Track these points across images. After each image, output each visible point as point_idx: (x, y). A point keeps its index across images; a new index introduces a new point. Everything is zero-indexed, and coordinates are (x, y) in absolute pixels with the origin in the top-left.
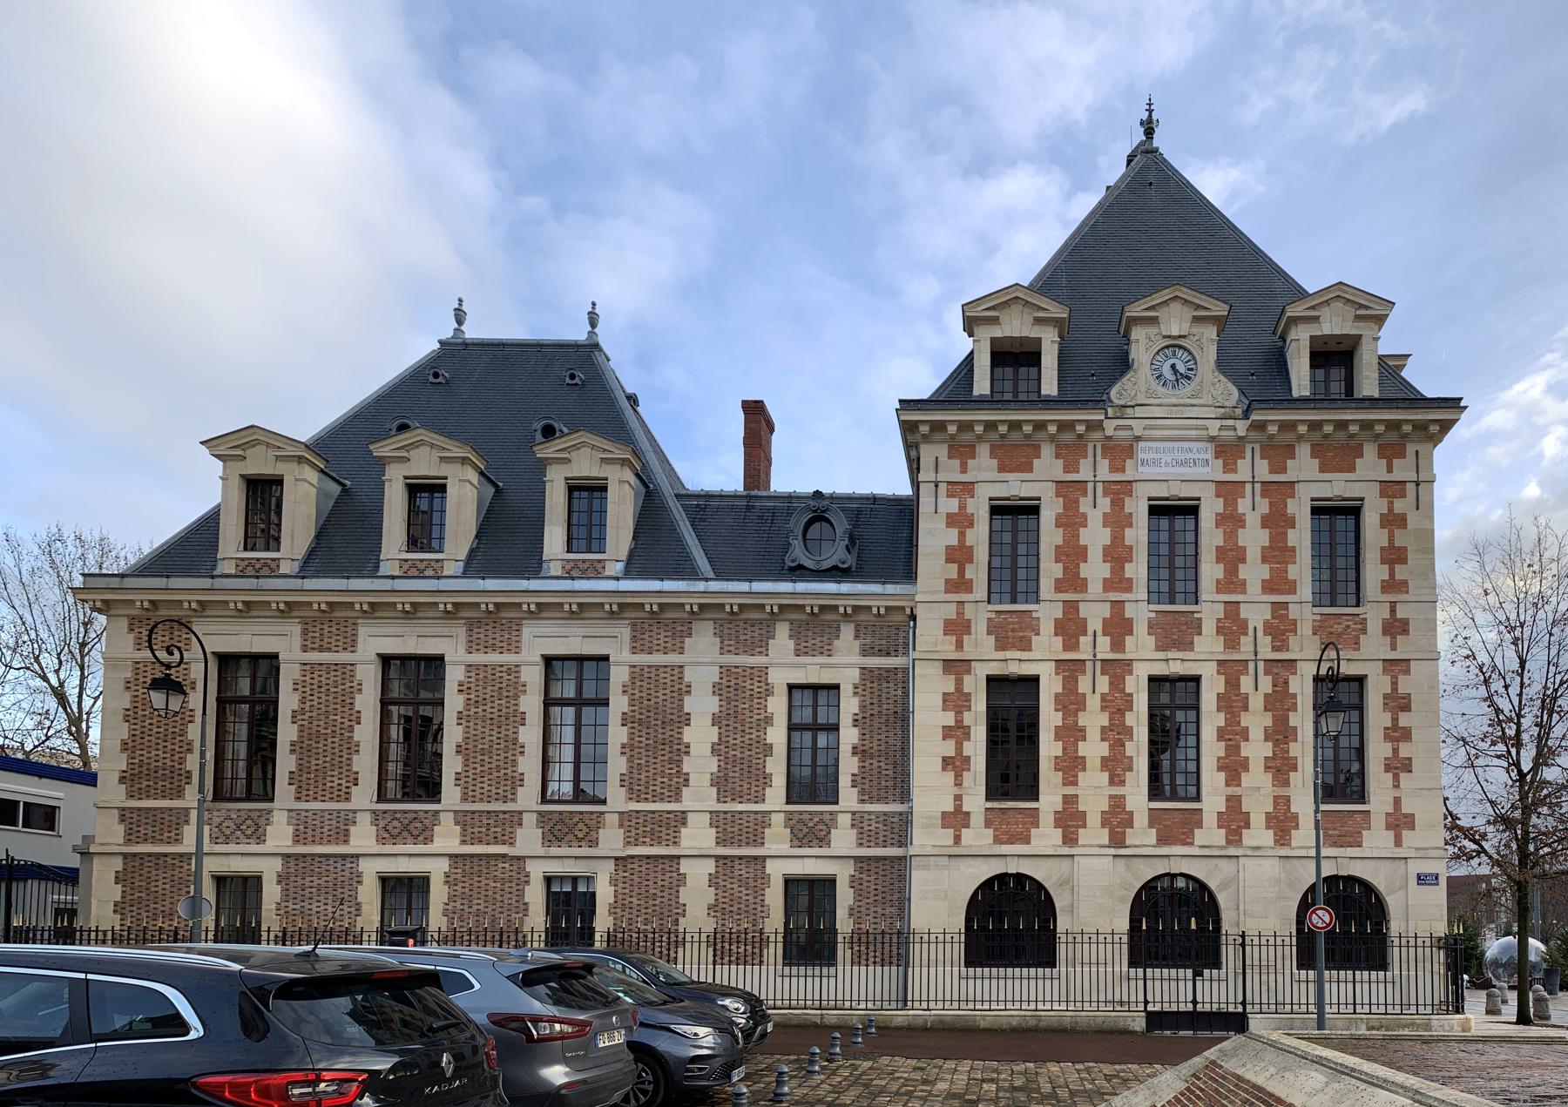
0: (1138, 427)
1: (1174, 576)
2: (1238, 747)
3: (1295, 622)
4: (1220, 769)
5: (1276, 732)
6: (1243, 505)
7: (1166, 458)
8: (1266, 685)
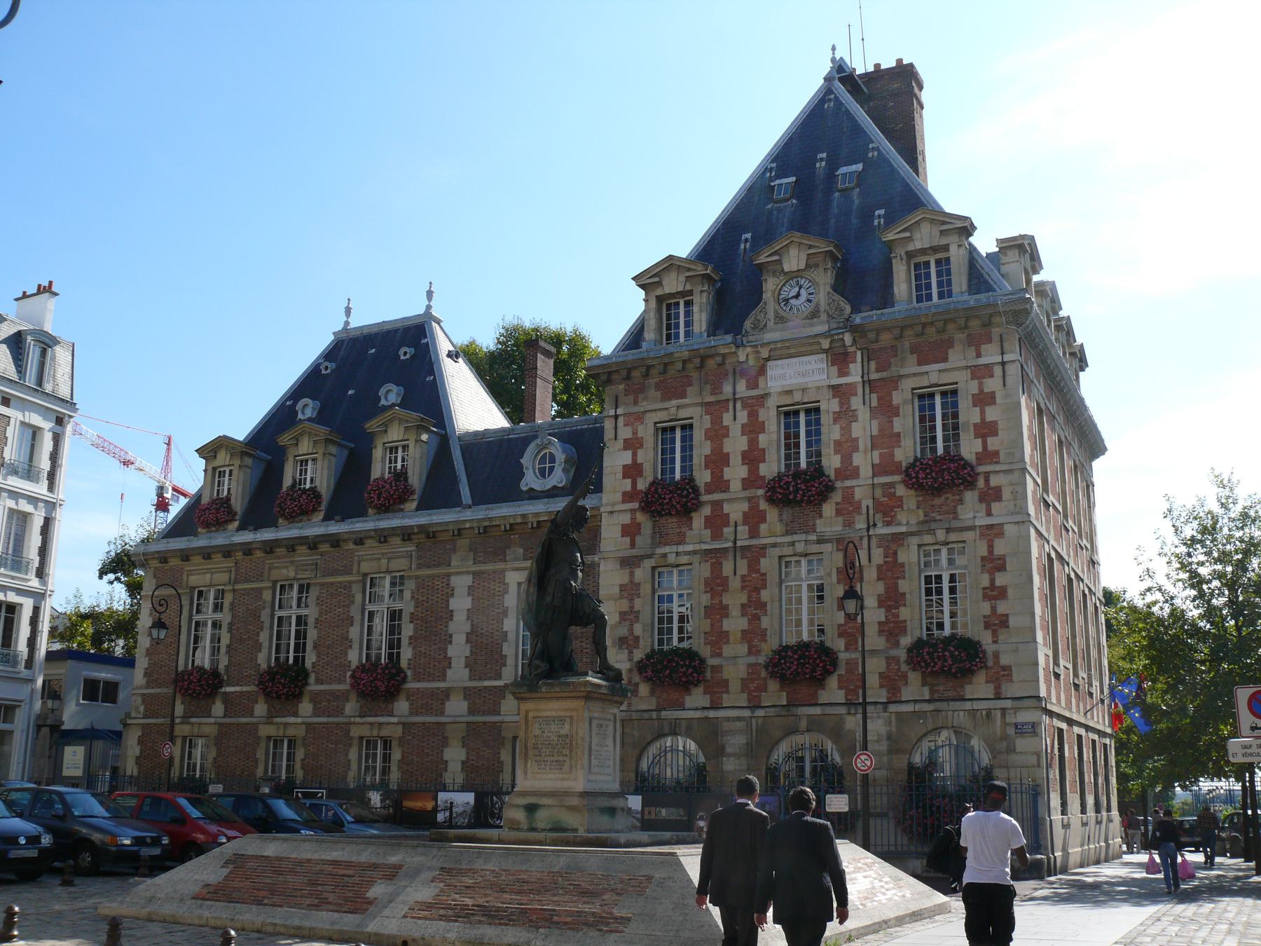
6: (856, 402)
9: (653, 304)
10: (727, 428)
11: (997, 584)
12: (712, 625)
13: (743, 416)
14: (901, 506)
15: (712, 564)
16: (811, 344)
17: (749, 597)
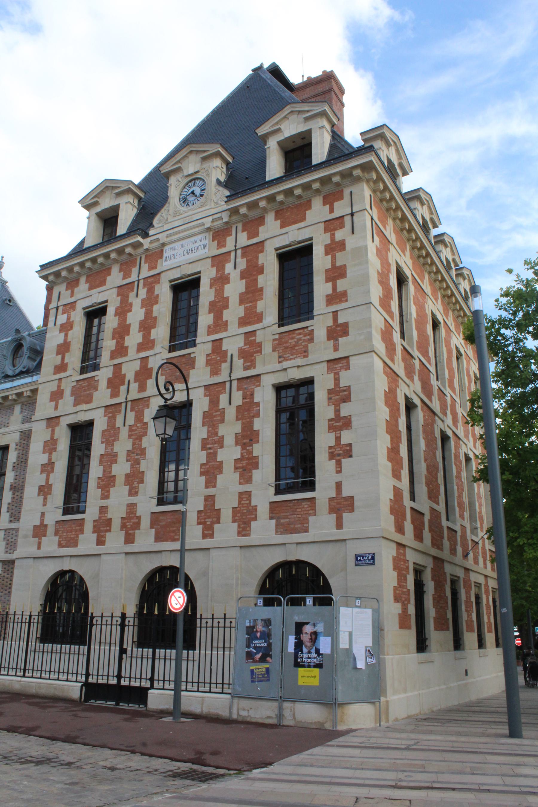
0: (162, 238)
1: (183, 330)
2: (215, 454)
3: (260, 345)
4: (202, 474)
5: (244, 437)
7: (180, 251)
8: (238, 398)
9: (94, 218)
10: (131, 305)
11: (342, 415)
12: (104, 471)
13: (143, 293)
14: (260, 352)
15: (109, 418)
16: (198, 226)
17: (134, 444)
